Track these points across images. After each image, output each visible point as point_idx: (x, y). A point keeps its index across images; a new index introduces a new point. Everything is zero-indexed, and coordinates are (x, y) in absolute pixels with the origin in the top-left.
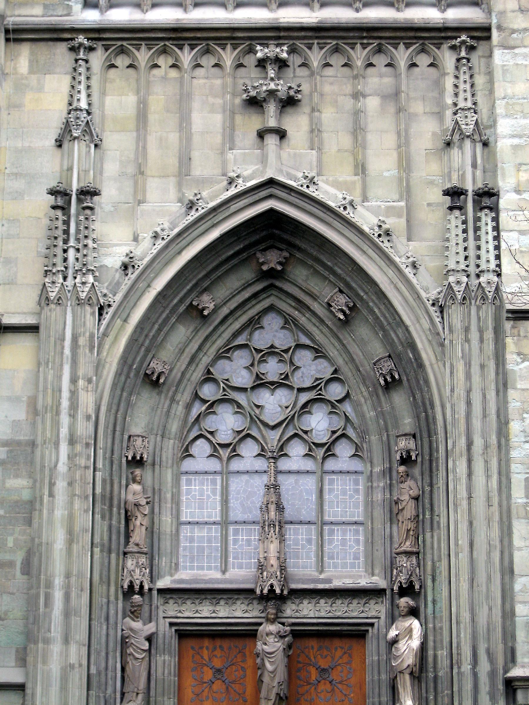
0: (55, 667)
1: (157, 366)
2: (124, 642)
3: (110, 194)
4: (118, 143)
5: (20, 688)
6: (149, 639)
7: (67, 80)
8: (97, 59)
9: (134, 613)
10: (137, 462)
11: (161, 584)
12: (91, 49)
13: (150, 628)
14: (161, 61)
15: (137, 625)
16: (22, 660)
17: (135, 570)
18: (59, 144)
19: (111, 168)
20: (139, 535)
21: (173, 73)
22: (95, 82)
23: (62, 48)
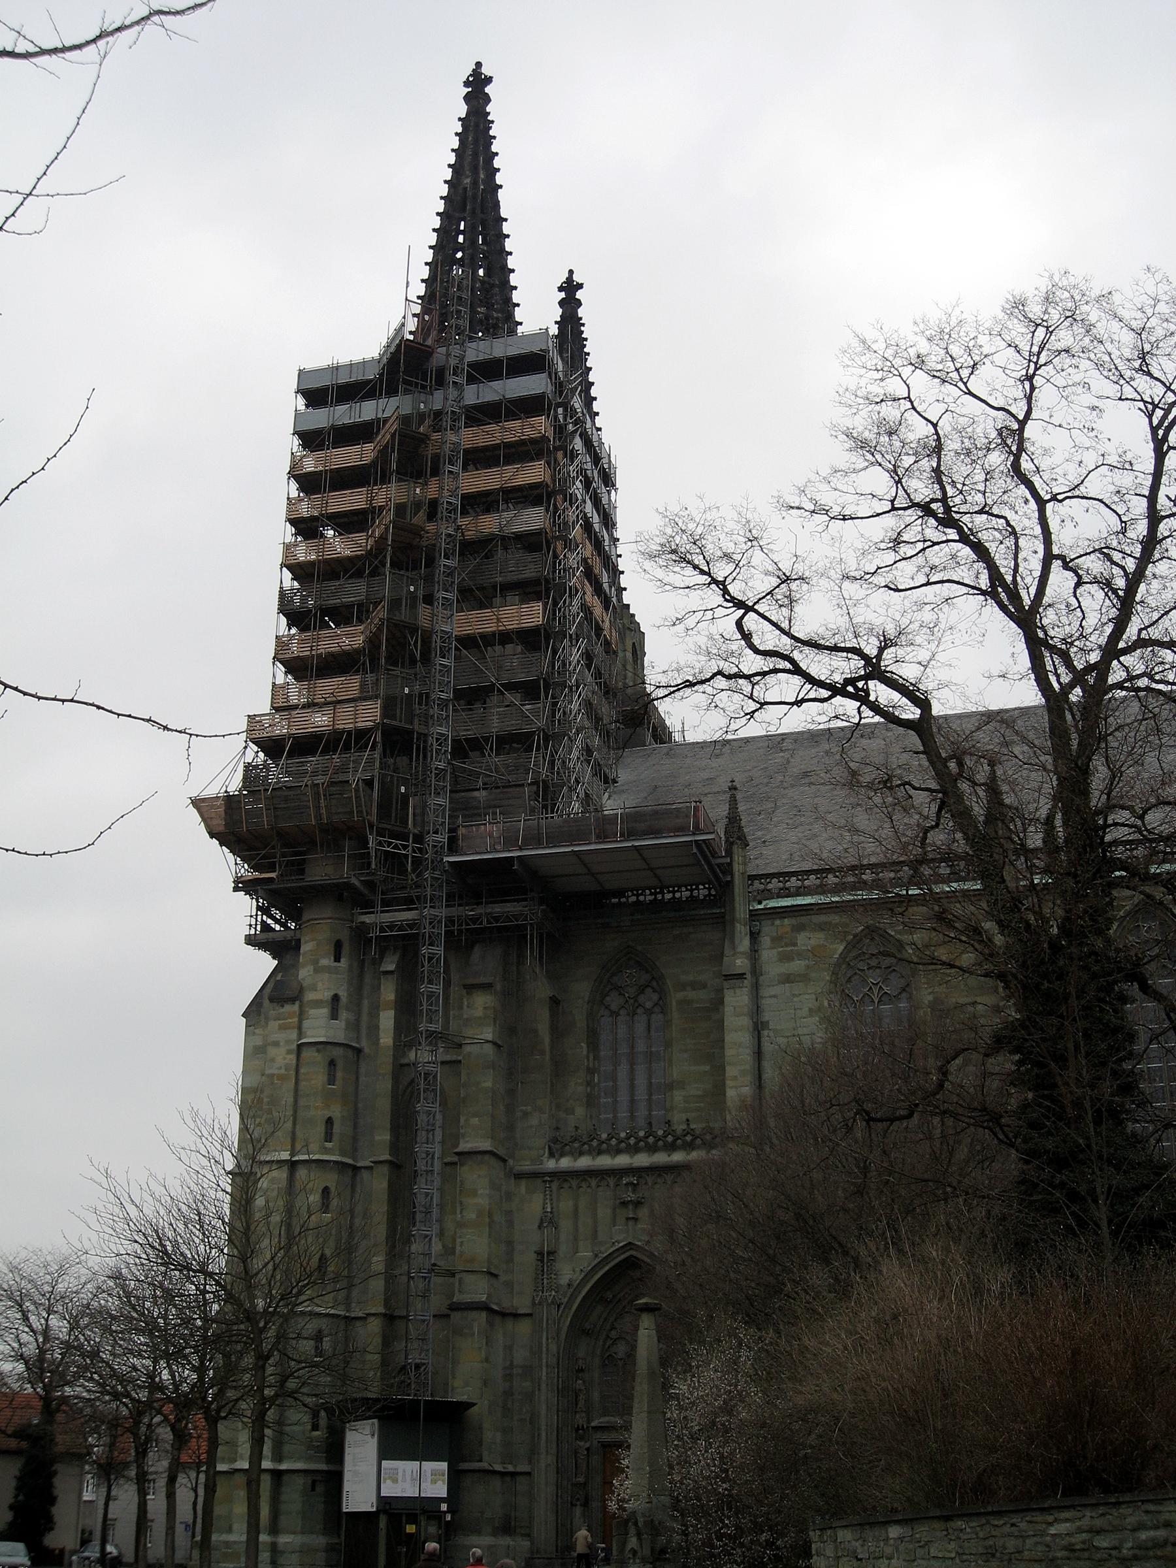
0: (543, 1464)
1: (587, 1326)
2: (576, 1452)
3: (563, 1249)
4: (566, 1225)
5: (529, 1474)
6: (588, 1449)
7: (542, 1196)
8: (555, 1186)
9: (581, 1438)
10: (581, 1370)
11: (593, 1424)
12: (551, 1181)
13: (588, 1445)
14: (583, 1184)
15: (582, 1444)
16: (530, 1462)
17: (580, 1419)
18: (539, 1227)
19: (563, 1237)
20: (581, 1404)
21: (589, 1190)
22: (555, 1196)
23: (540, 1180)
